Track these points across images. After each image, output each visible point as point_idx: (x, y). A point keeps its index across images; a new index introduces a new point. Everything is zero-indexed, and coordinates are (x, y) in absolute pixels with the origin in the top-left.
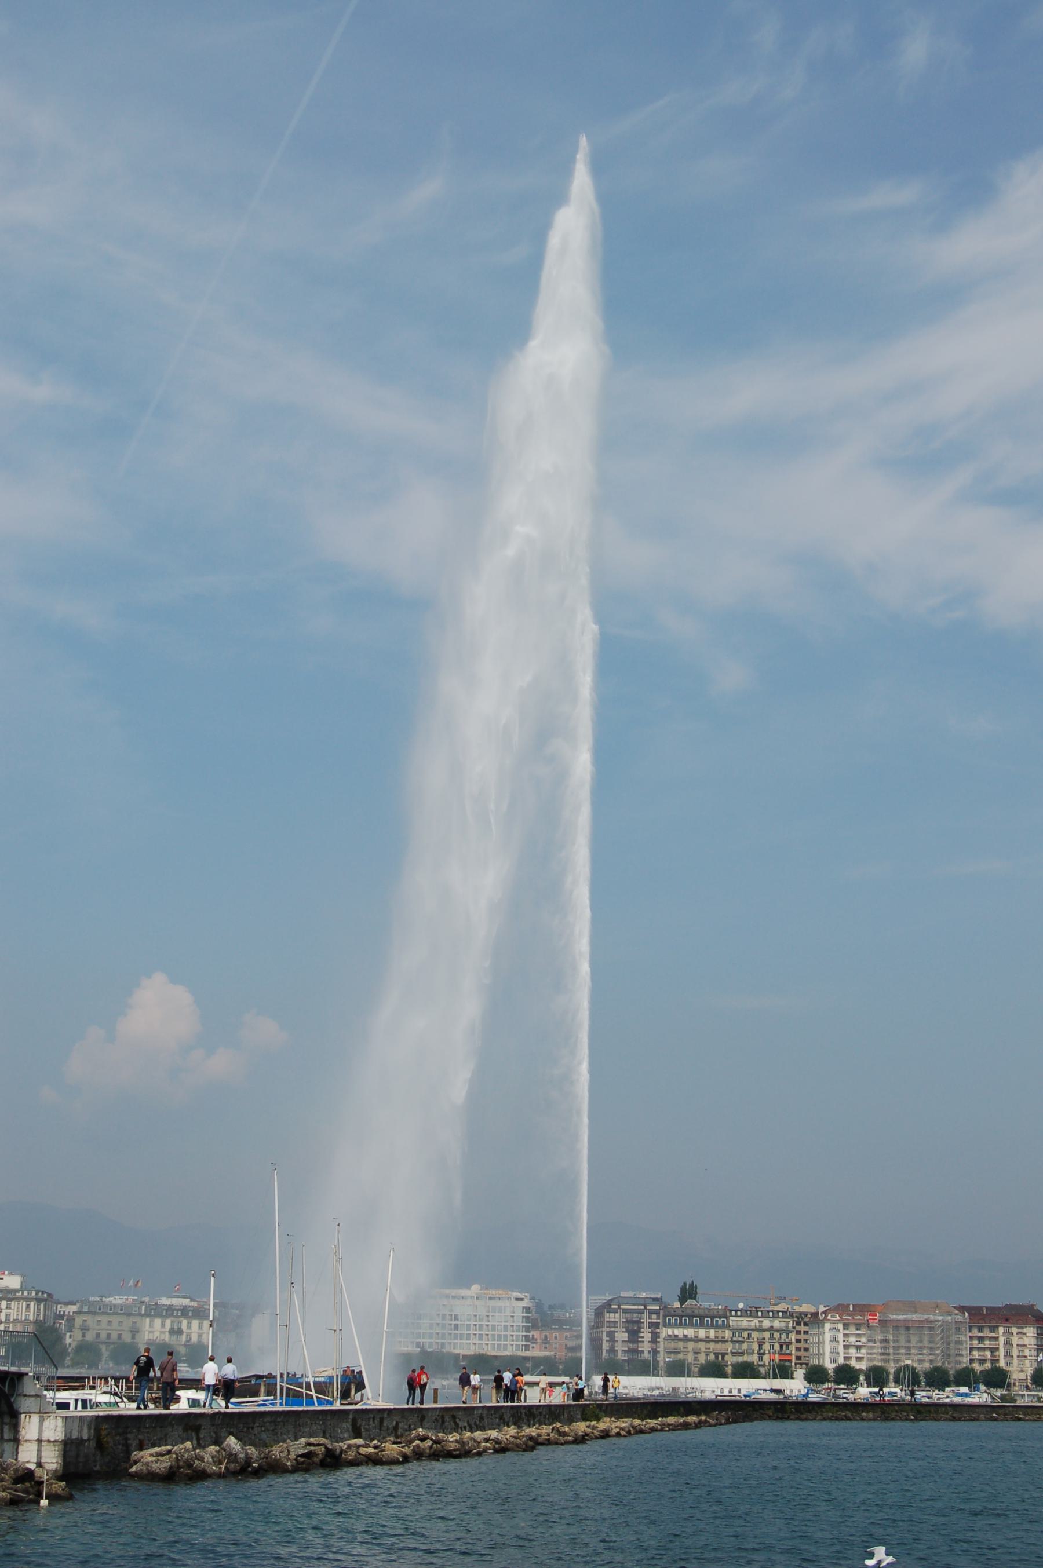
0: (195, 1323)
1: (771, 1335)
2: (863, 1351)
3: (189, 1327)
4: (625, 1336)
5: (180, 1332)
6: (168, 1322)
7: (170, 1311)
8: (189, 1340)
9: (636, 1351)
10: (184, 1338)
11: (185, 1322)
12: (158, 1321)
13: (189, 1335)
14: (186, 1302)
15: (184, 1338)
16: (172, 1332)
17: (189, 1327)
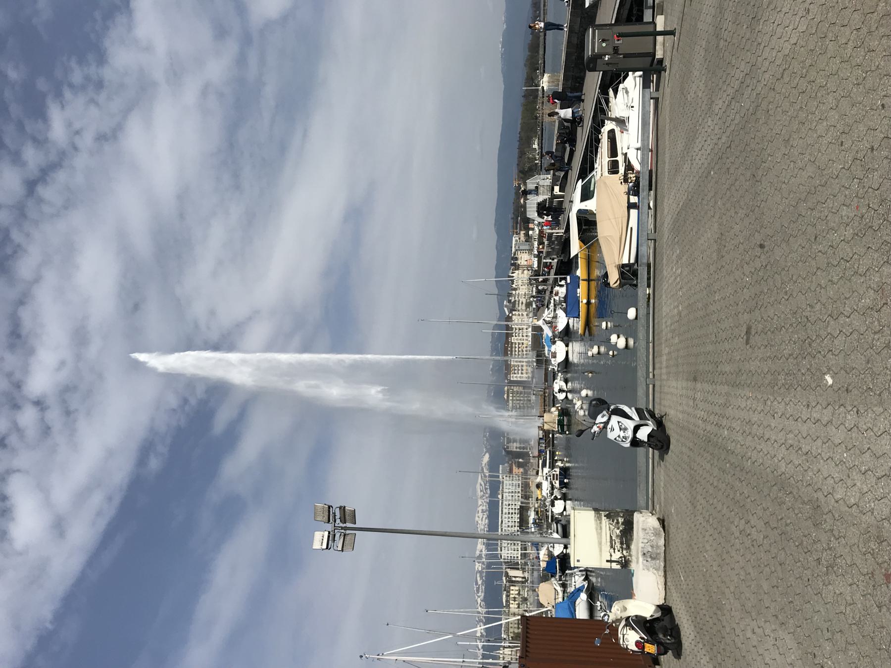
0: (511, 592)
1: (515, 396)
2: (519, 368)
3: (513, 594)
4: (515, 444)
5: (515, 598)
6: (511, 602)
7: (507, 601)
8: (517, 594)
9: (496, 556)
10: (517, 596)
11: (511, 596)
12: (511, 606)
13: (515, 595)
14: (504, 596)
15: (517, 596)
16: (515, 601)
17: (513, 594)
